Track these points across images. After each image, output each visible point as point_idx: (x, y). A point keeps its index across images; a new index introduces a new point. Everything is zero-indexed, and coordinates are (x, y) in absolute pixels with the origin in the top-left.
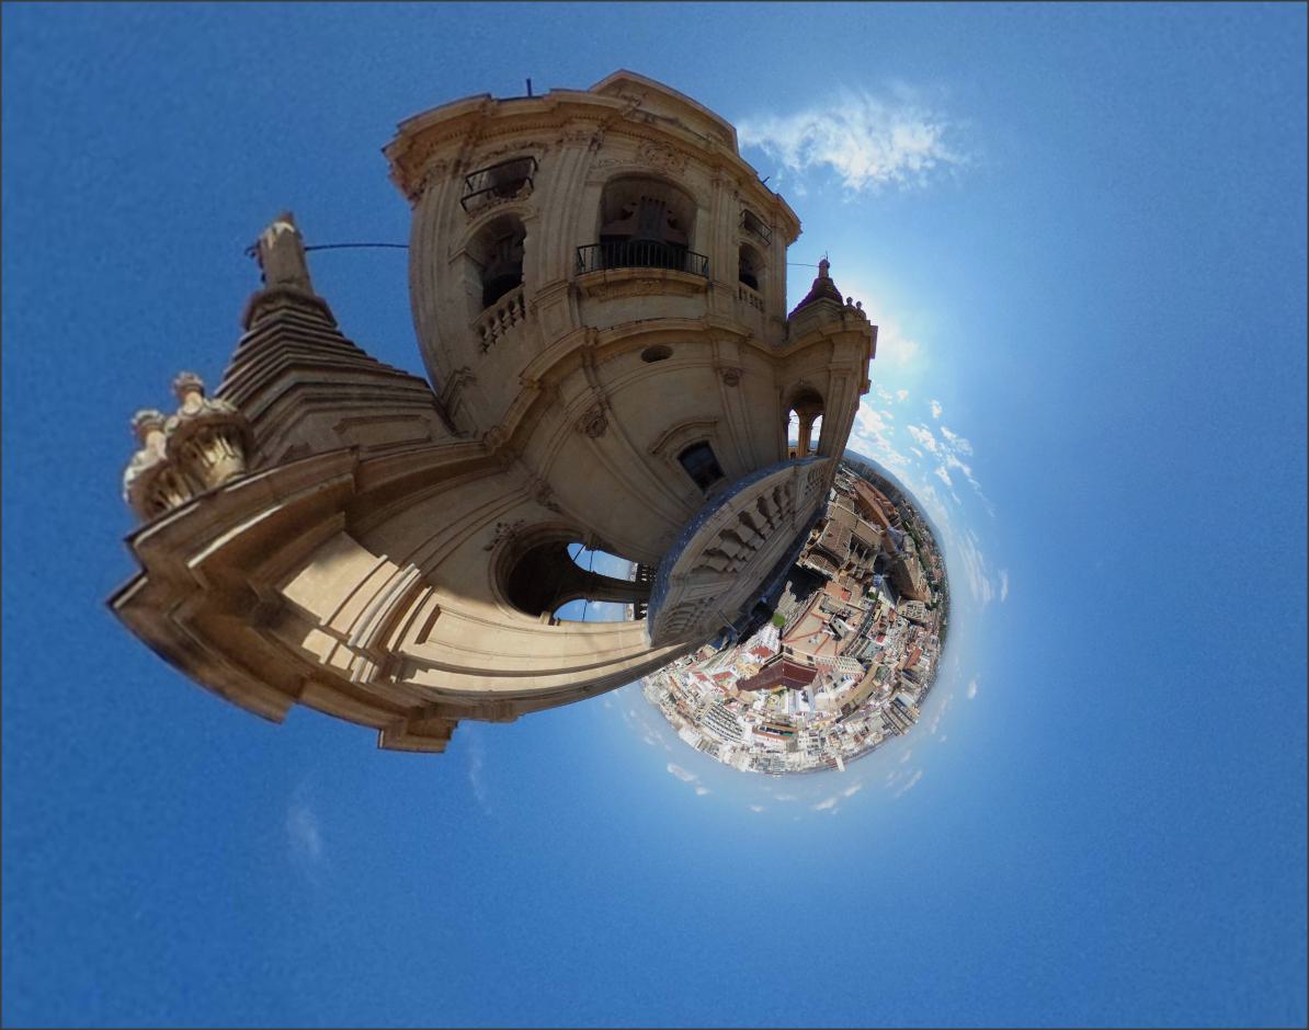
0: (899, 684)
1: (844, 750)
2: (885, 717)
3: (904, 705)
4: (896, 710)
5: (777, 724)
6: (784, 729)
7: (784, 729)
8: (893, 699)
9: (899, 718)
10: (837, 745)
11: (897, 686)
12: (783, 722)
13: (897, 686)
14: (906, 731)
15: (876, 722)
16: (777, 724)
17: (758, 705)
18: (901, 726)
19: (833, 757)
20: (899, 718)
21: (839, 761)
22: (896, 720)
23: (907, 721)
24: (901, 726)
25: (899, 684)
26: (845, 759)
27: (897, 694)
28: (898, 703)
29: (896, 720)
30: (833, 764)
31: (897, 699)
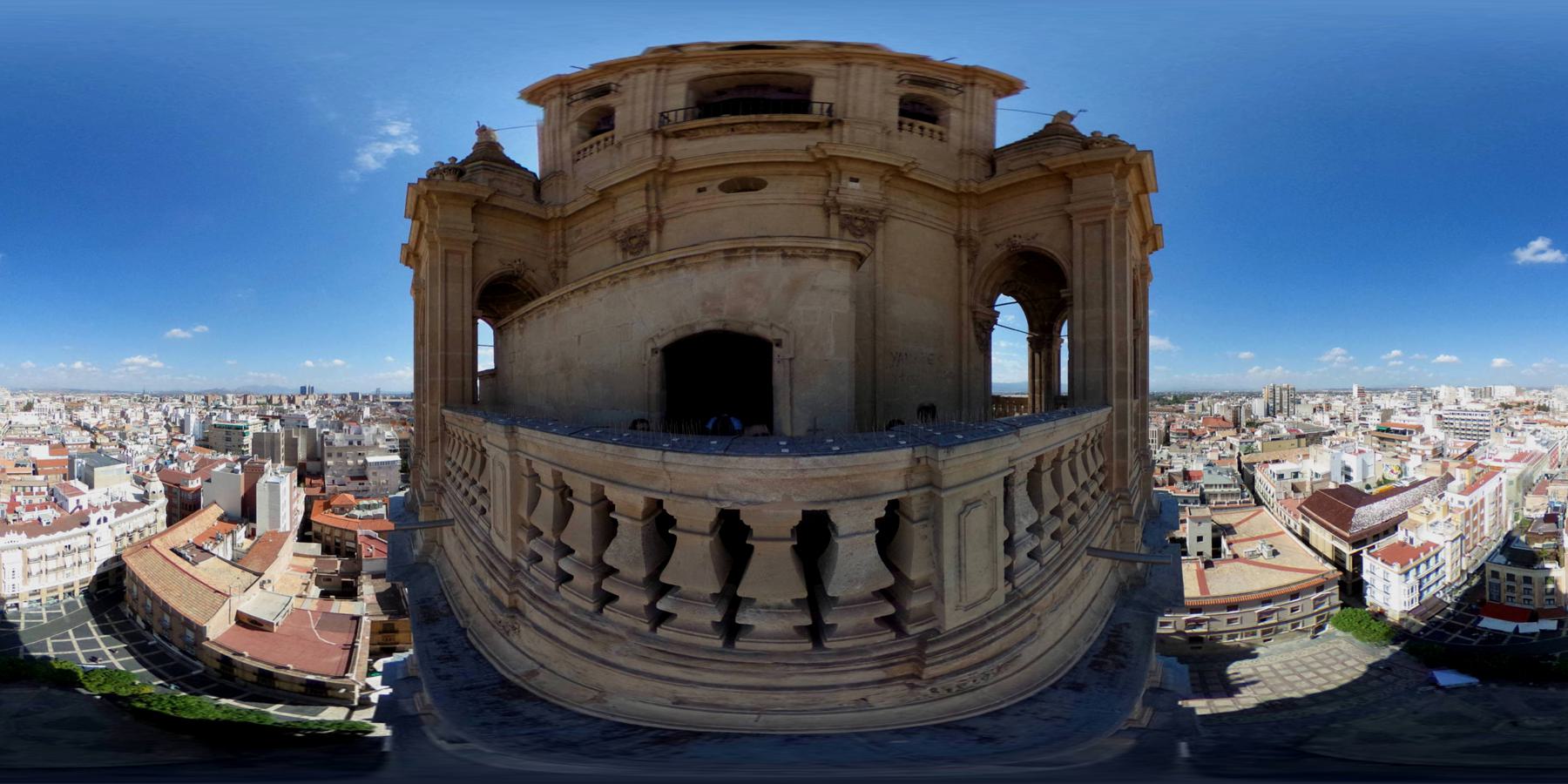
0: (1249, 424)
1: (1345, 402)
2: (1291, 410)
3: (1268, 405)
4: (1278, 408)
5: (1393, 440)
6: (1388, 435)
7: (1388, 435)
8: (1269, 419)
9: (1281, 399)
10: (1349, 409)
11: (1253, 424)
12: (1387, 443)
13: (1253, 424)
14: (1285, 385)
15: (1304, 410)
16: (1393, 440)
17: (1415, 460)
18: (1285, 393)
19: (1359, 399)
20: (1281, 399)
21: (1355, 393)
22: (1285, 400)
23: (1278, 392)
24: (1285, 393)
25: (1249, 424)
26: (1348, 393)
27: (1262, 418)
28: (1270, 412)
29: (1285, 400)
30: (1361, 392)
31: (1268, 414)
